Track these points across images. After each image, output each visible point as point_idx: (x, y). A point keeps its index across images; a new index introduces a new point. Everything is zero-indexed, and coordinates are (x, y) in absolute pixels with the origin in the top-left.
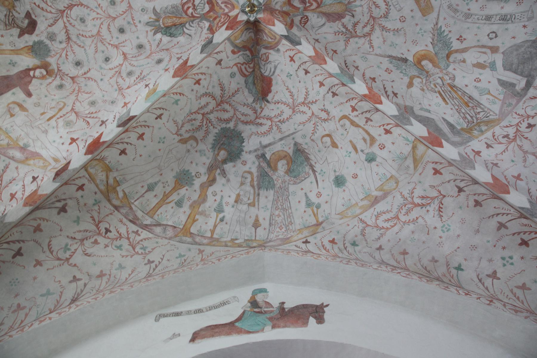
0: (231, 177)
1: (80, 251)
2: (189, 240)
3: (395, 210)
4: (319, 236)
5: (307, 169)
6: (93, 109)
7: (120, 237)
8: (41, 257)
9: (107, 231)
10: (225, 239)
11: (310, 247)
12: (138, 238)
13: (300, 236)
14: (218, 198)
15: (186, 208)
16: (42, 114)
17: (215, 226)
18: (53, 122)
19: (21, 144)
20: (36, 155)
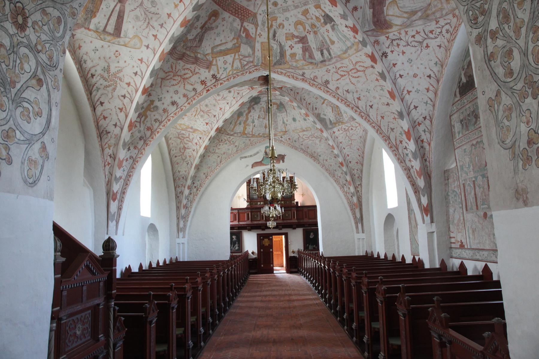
0: (256, 109)
1: (217, 149)
2: (245, 136)
3: (309, 136)
4: (285, 136)
5: (284, 110)
6: (207, 109)
7: (226, 140)
8: (209, 154)
9: (222, 140)
10: (256, 134)
11: (283, 139)
12: (230, 139)
13: (280, 134)
14: (252, 117)
15: (242, 124)
16: (192, 115)
17: (253, 129)
18: (196, 116)
19: (190, 127)
20: (196, 130)
